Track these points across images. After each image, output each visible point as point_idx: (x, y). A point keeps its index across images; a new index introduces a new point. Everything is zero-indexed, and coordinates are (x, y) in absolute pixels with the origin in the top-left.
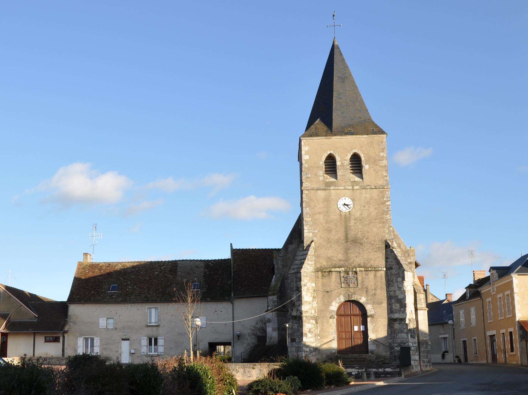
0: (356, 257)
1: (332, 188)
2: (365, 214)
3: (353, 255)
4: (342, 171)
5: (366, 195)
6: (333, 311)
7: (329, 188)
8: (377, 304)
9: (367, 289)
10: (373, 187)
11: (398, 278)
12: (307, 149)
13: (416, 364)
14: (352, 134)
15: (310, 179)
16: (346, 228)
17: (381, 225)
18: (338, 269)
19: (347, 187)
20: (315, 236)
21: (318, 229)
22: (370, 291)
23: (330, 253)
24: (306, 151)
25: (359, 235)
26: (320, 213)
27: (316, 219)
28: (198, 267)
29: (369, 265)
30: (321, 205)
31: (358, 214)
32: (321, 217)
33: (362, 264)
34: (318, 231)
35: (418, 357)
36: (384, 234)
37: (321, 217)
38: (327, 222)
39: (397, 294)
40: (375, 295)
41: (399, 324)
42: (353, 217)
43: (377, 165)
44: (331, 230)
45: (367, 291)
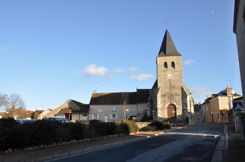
2: (176, 79)
5: (176, 73)
14: (172, 56)
18: (168, 95)
19: (171, 71)
23: (165, 90)
25: (174, 85)
26: (163, 79)
30: (163, 76)
31: (173, 79)
32: (163, 80)
34: (162, 84)
37: (163, 80)
38: (165, 81)
40: (178, 102)
42: (172, 80)
44: (166, 84)
45: (176, 101)
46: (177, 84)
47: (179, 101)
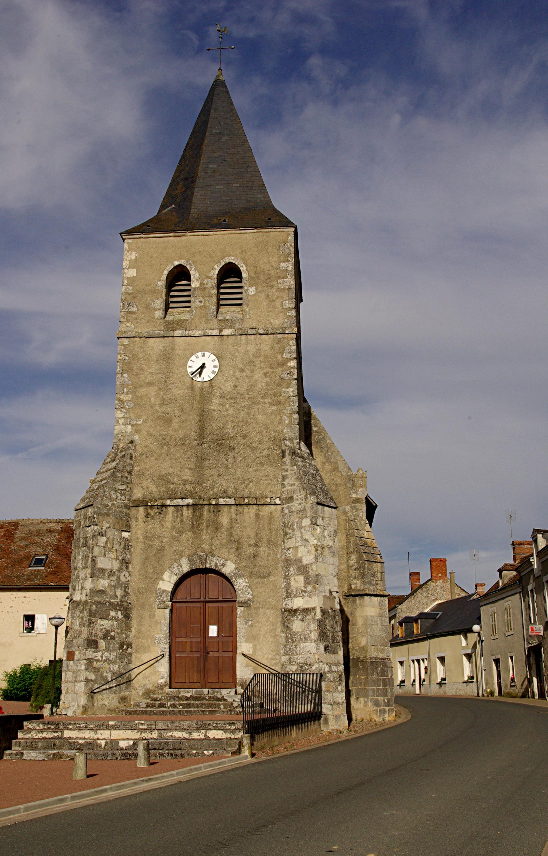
0: (219, 475)
1: (177, 333)
2: (243, 387)
3: (213, 472)
4: (202, 299)
5: (249, 346)
6: (164, 591)
7: (171, 333)
8: (260, 577)
9: (239, 543)
10: (261, 331)
11: (302, 518)
12: (134, 258)
13: (336, 713)
14: (227, 227)
15: (134, 316)
16: (201, 415)
17: (275, 408)
18: (179, 502)
19: (210, 332)
20: (137, 431)
21: (144, 418)
22: (245, 548)
23: (166, 467)
24: (130, 261)
25: (229, 430)
26: (150, 384)
27: (141, 397)
28: (50, 531)
29: (246, 493)
30: (155, 368)
31: (228, 387)
32: (152, 391)
33: (230, 492)
34: (144, 421)
35: (343, 695)
36: (280, 428)
37: (152, 391)
38: (162, 405)
39: (300, 555)
40: (255, 556)
41: (302, 620)
42: (217, 393)
43: (272, 287)
44: (169, 421)
45: (237, 549)
46: (247, 423)
47: (257, 545)
